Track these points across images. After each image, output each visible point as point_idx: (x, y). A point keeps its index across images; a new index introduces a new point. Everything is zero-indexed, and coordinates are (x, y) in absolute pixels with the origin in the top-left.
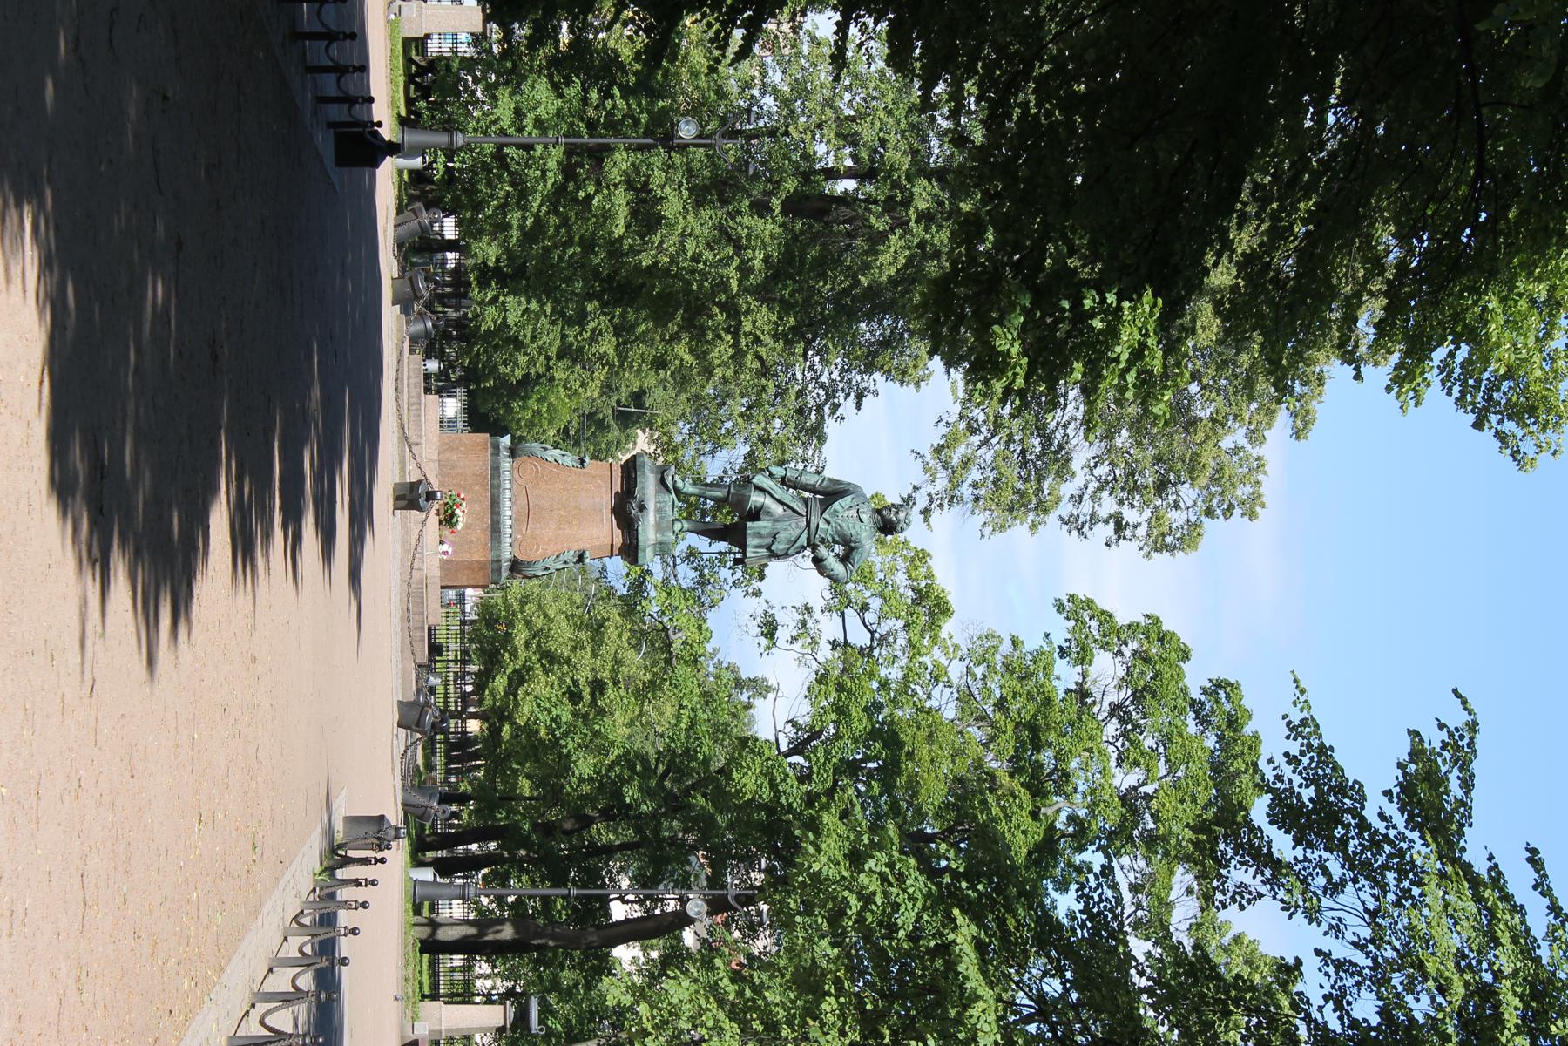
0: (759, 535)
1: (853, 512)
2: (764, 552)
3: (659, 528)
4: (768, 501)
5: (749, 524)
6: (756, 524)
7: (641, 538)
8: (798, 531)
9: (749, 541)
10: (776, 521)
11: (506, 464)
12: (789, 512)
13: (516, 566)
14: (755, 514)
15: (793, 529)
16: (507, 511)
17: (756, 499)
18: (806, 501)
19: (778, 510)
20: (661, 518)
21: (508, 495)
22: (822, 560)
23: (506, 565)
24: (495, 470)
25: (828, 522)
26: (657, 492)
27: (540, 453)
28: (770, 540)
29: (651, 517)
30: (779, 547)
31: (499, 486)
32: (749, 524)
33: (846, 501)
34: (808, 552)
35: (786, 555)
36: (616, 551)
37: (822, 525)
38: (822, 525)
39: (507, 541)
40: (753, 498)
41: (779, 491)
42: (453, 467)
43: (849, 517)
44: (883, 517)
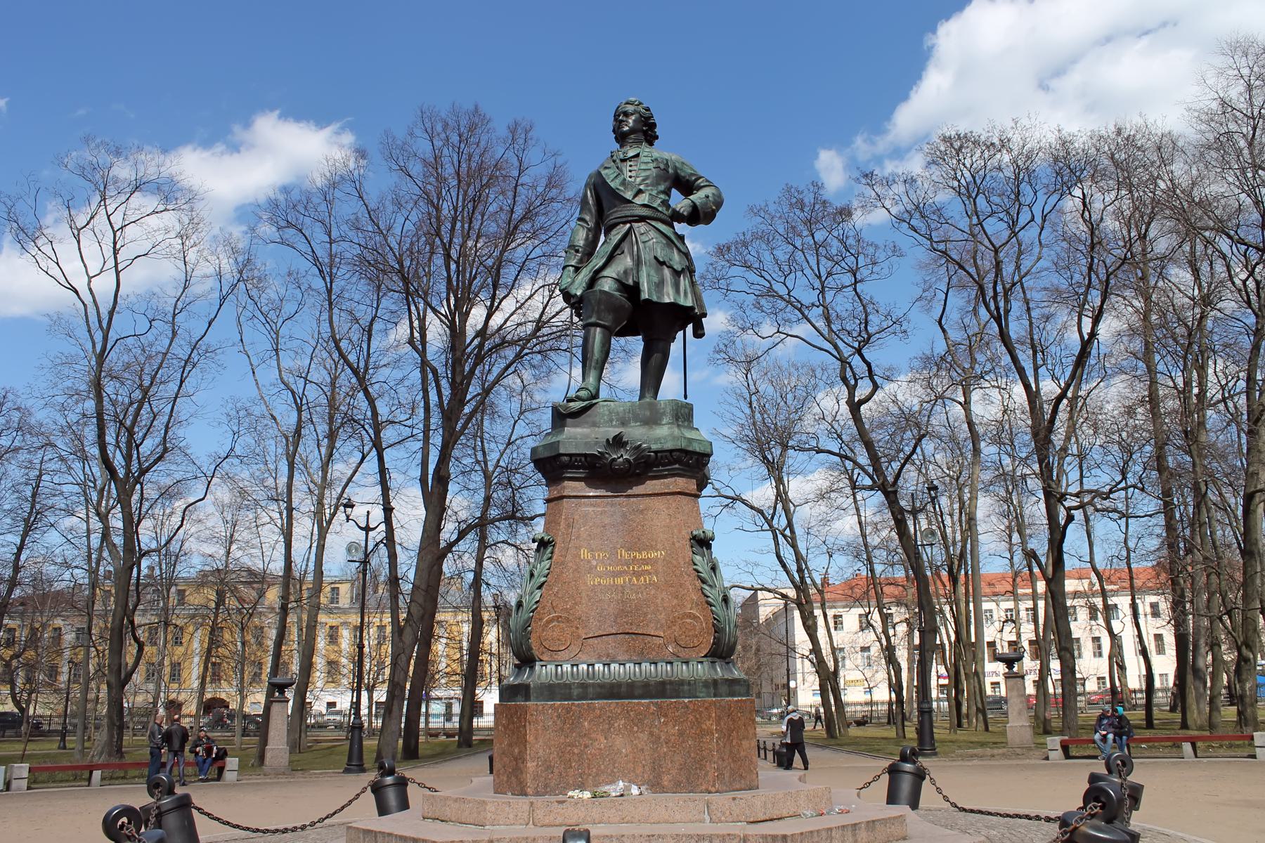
0: (660, 285)
1: (626, 167)
2: (684, 282)
3: (652, 420)
4: (610, 272)
5: (645, 295)
6: (645, 286)
7: (669, 446)
8: (652, 234)
9: (667, 300)
10: (638, 262)
11: (544, 672)
12: (625, 246)
13: (721, 652)
14: (631, 291)
15: (648, 239)
16: (621, 671)
17: (606, 285)
18: (608, 230)
19: (625, 262)
20: (636, 418)
21: (599, 667)
22: (694, 206)
23: (719, 672)
24: (555, 691)
25: (640, 192)
26: (594, 425)
27: (524, 614)
28: (667, 272)
29: (636, 433)
30: (677, 260)
31: (584, 686)
32: (645, 295)
33: (609, 175)
34: (680, 228)
35: (686, 255)
36: (691, 485)
37: (643, 199)
38: (643, 199)
39: (682, 671)
40: (606, 288)
41: (597, 262)
42: (549, 768)
43: (636, 175)
44: (632, 131)
